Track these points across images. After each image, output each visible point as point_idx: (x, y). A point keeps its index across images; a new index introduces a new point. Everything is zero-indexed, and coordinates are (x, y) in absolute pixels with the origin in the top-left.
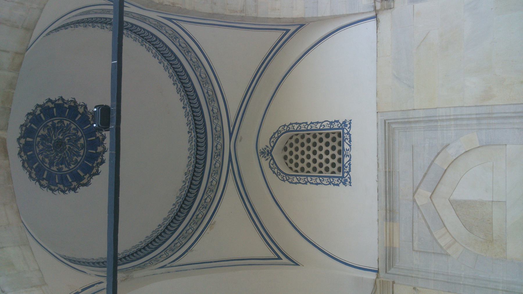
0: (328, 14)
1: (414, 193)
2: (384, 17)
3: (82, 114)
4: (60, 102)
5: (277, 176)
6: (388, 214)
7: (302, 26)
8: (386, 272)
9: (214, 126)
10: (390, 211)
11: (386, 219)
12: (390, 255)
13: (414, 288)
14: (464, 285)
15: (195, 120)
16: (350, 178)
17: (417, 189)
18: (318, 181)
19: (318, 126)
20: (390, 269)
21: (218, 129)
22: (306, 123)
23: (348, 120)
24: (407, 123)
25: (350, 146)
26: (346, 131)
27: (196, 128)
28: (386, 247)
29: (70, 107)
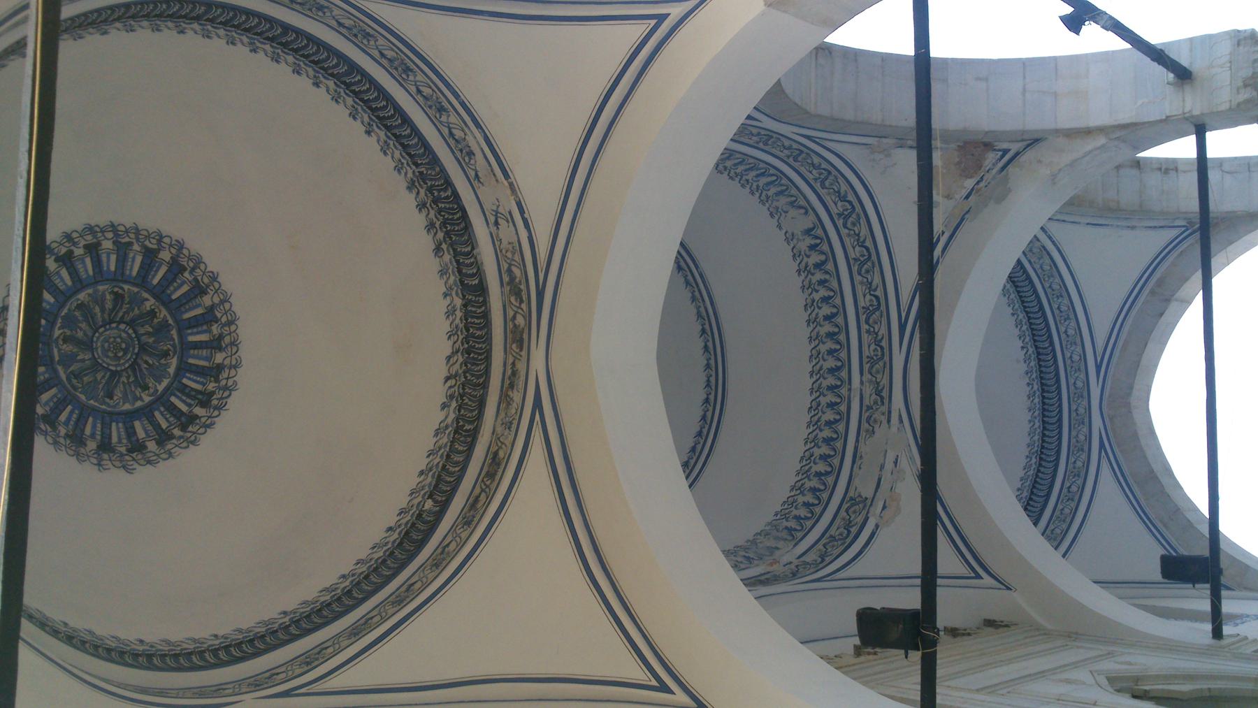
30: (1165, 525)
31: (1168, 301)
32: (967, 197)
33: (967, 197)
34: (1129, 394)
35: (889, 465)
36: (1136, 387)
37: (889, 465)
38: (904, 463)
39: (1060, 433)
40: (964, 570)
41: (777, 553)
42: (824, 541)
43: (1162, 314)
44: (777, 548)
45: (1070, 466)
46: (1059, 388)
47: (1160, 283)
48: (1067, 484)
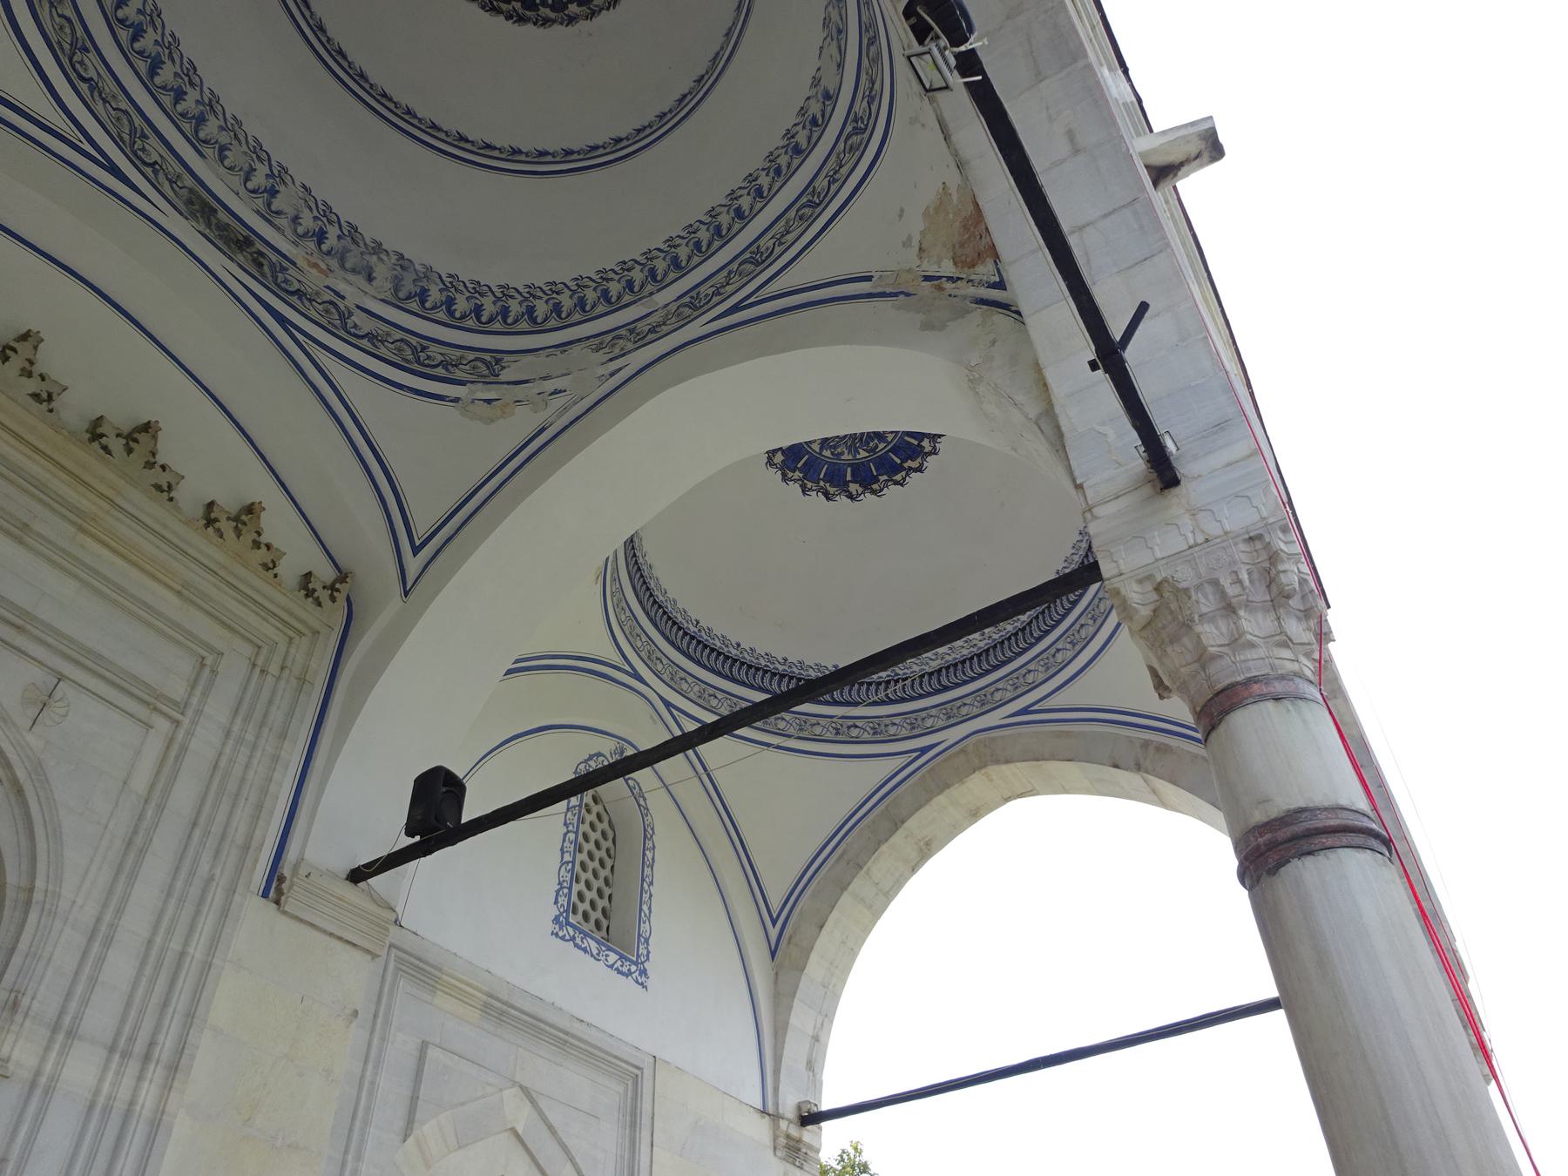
0: (793, 1020)
1: (525, 1091)
2: (760, 1130)
3: (846, 483)
4: (898, 477)
5: (586, 761)
6: (499, 1005)
7: (773, 954)
8: (391, 946)
9: (690, 679)
10: (503, 1013)
11: (491, 996)
12: (423, 970)
13: (355, 1014)
14: (344, 1164)
15: (713, 650)
16: (563, 938)
17: (533, 1102)
18: (567, 857)
19: (645, 908)
20: (399, 960)
21: (685, 686)
22: (652, 883)
23: (649, 983)
24: (632, 1118)
25: (611, 967)
26: (633, 968)
27: (699, 642)
28: (440, 970)
29: (876, 480)
30: (841, 857)
31: (1138, 768)
32: (927, 278)
33: (927, 278)
34: (998, 762)
35: (549, 386)
36: (1011, 766)
37: (549, 386)
38: (559, 401)
39: (929, 694)
40: (421, 530)
41: (360, 281)
42: (414, 340)
43: (1116, 766)
44: (370, 279)
45: (887, 721)
46: (988, 672)
47: (1162, 749)
48: (859, 723)
